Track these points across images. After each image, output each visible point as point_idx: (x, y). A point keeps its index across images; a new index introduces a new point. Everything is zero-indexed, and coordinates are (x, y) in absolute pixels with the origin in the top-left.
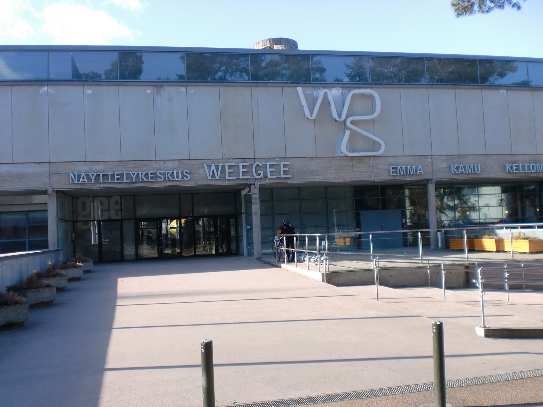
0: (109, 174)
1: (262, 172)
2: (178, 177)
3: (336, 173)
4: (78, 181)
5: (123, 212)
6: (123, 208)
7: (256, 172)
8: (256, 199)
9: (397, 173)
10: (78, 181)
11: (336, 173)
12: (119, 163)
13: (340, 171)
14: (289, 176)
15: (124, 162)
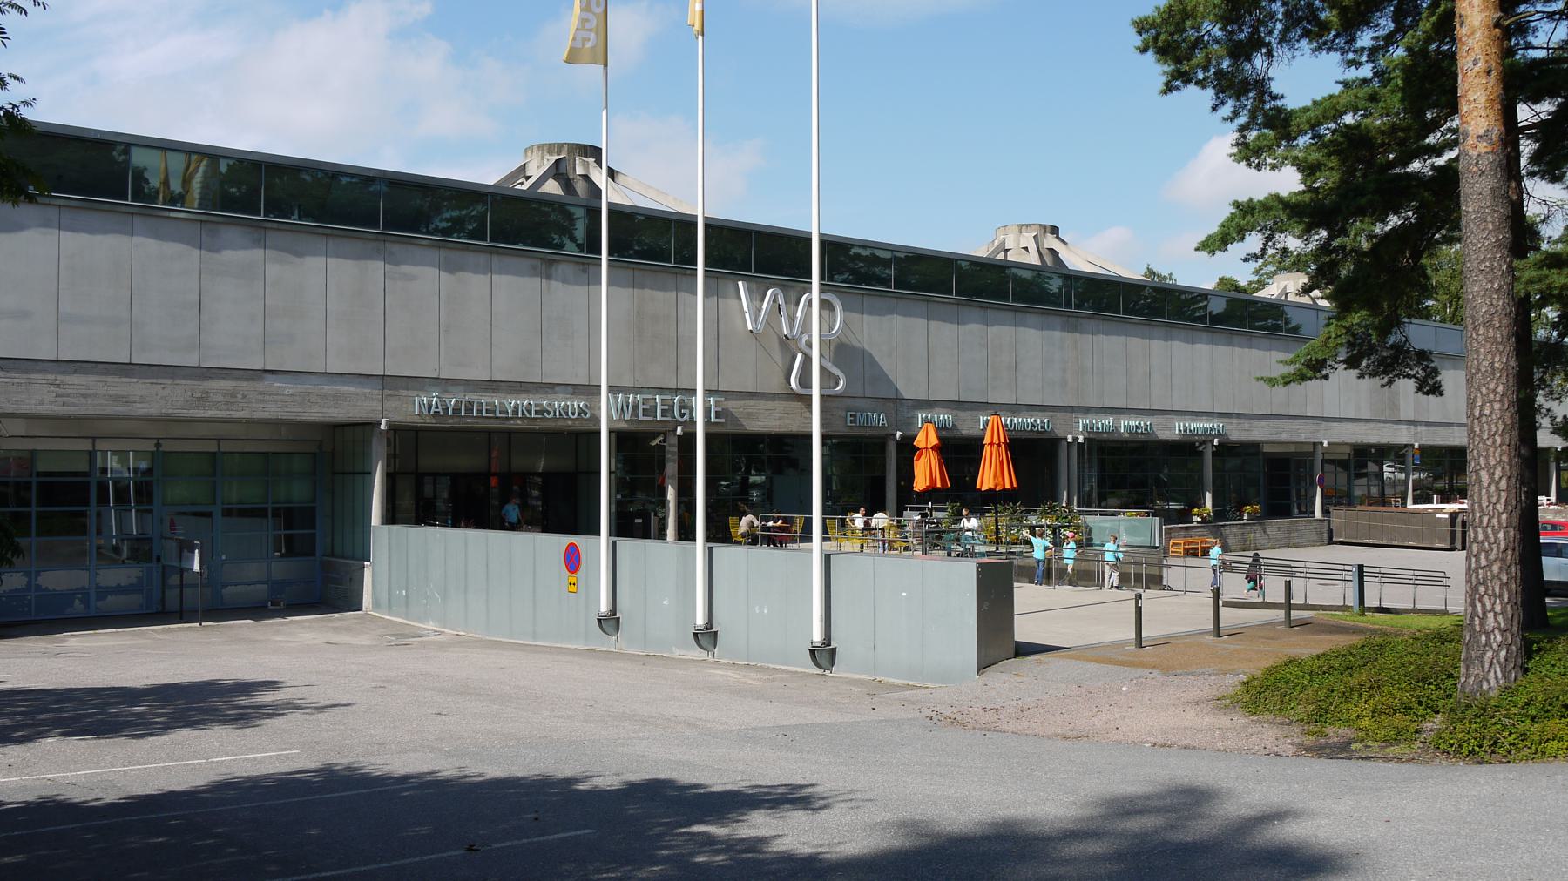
0: (476, 401)
1: (687, 411)
2: (573, 414)
3: (780, 418)
4: (429, 411)
5: (397, 460)
6: (397, 452)
7: (680, 411)
8: (672, 453)
9: (855, 423)
10: (429, 411)
11: (780, 418)
12: (488, 383)
13: (786, 415)
14: (722, 420)
15: (494, 384)
